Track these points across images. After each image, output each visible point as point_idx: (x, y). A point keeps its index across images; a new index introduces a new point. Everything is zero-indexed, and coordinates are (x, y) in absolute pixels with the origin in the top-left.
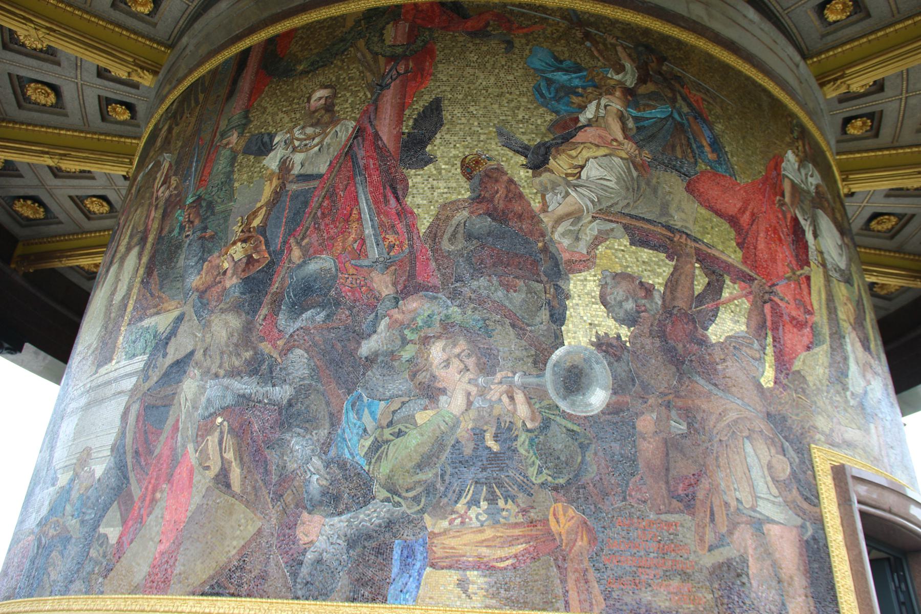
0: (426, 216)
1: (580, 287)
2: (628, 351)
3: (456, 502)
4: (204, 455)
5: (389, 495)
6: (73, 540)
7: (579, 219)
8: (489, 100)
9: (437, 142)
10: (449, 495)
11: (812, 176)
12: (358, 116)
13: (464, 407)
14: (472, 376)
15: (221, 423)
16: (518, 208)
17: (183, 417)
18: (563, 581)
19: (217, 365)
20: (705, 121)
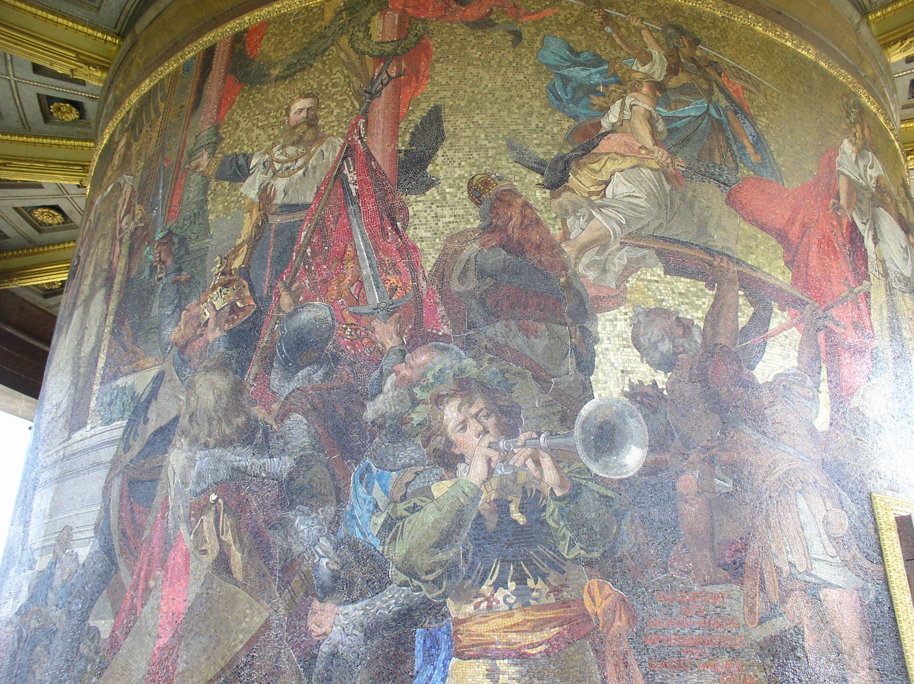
0: (431, 250)
1: (609, 328)
2: (666, 401)
3: (482, 583)
4: (198, 535)
5: (408, 579)
6: (60, 634)
7: (605, 247)
8: (497, 106)
9: (439, 160)
10: (473, 577)
11: (871, 168)
12: (346, 132)
13: (484, 475)
14: (492, 439)
15: (216, 501)
16: (535, 237)
17: (173, 494)
18: (602, 667)
19: (206, 433)
20: (747, 115)
